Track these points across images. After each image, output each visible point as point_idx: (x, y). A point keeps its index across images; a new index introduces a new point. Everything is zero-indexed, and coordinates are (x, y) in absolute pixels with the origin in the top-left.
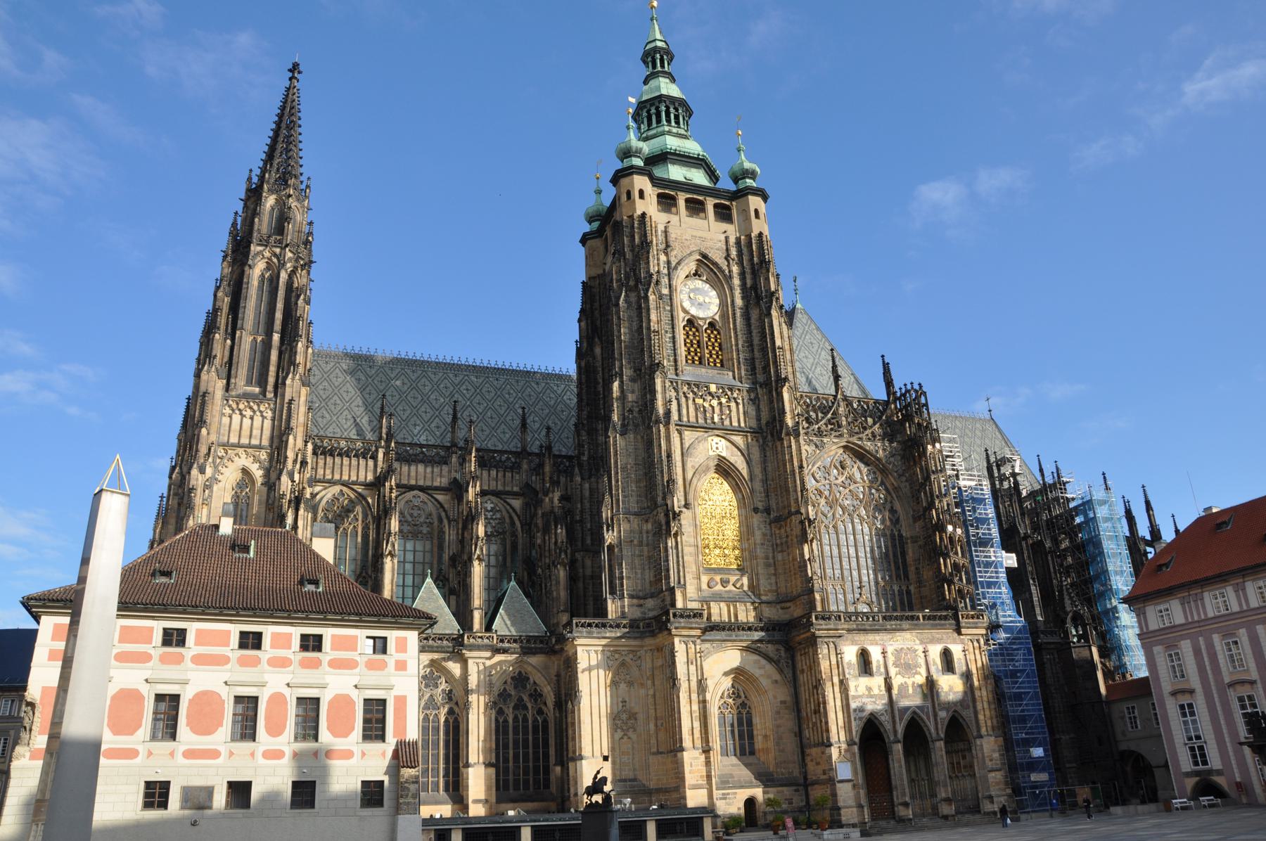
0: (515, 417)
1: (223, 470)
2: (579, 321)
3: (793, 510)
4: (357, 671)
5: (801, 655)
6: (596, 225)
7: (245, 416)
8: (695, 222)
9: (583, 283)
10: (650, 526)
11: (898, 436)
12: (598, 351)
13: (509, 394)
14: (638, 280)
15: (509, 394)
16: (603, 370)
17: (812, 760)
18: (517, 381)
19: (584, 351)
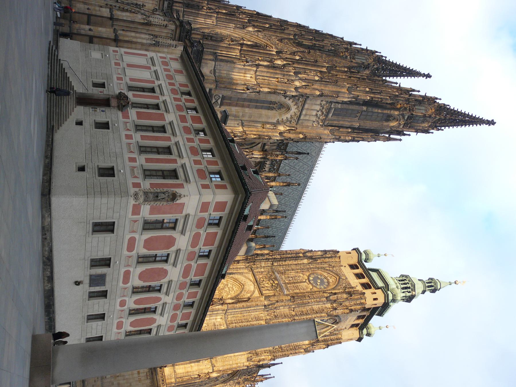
0: (281, 199)
1: (291, 100)
2: (321, 251)
3: (214, 368)
4: (169, 322)
5: (147, 374)
6: (364, 257)
7: (318, 111)
8: (355, 317)
9: (338, 252)
10: (219, 320)
11: (238, 386)
12: (305, 261)
13: (293, 194)
14: (336, 309)
15: (293, 194)
16: (296, 264)
17: (95, 381)
18: (298, 195)
19: (307, 254)
